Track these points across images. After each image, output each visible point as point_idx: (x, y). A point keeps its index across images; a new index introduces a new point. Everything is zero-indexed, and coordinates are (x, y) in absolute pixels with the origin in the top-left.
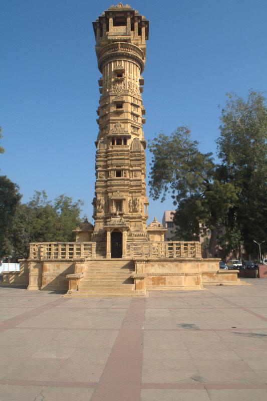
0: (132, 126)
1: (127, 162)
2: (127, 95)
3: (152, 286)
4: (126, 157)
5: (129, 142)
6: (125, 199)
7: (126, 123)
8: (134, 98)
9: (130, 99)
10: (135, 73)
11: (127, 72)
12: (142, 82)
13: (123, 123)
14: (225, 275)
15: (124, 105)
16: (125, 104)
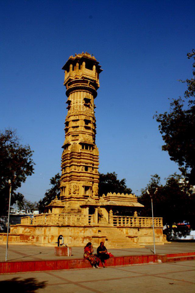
0: (72, 136)
1: (66, 161)
2: (70, 116)
3: (36, 242)
4: (66, 159)
5: (70, 147)
6: (65, 187)
7: (69, 135)
8: (75, 115)
9: (72, 118)
10: (79, 97)
11: (72, 100)
12: (87, 101)
13: (68, 136)
14: (95, 238)
15: (70, 123)
16: (70, 122)
